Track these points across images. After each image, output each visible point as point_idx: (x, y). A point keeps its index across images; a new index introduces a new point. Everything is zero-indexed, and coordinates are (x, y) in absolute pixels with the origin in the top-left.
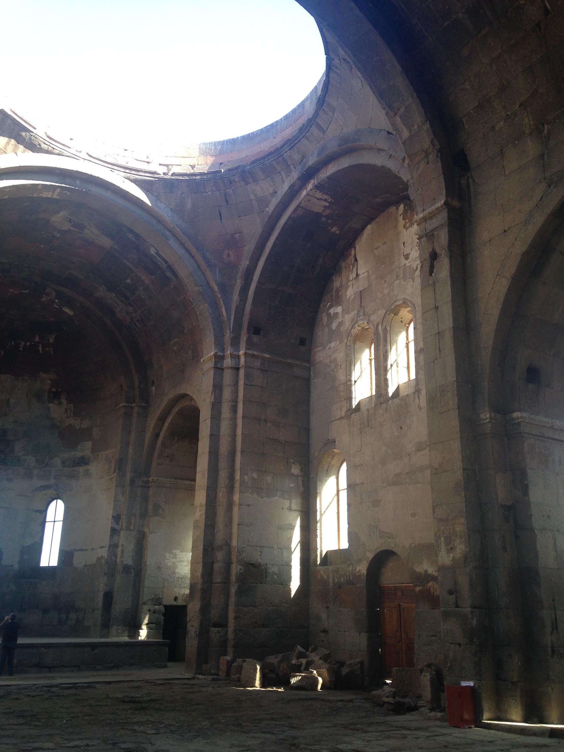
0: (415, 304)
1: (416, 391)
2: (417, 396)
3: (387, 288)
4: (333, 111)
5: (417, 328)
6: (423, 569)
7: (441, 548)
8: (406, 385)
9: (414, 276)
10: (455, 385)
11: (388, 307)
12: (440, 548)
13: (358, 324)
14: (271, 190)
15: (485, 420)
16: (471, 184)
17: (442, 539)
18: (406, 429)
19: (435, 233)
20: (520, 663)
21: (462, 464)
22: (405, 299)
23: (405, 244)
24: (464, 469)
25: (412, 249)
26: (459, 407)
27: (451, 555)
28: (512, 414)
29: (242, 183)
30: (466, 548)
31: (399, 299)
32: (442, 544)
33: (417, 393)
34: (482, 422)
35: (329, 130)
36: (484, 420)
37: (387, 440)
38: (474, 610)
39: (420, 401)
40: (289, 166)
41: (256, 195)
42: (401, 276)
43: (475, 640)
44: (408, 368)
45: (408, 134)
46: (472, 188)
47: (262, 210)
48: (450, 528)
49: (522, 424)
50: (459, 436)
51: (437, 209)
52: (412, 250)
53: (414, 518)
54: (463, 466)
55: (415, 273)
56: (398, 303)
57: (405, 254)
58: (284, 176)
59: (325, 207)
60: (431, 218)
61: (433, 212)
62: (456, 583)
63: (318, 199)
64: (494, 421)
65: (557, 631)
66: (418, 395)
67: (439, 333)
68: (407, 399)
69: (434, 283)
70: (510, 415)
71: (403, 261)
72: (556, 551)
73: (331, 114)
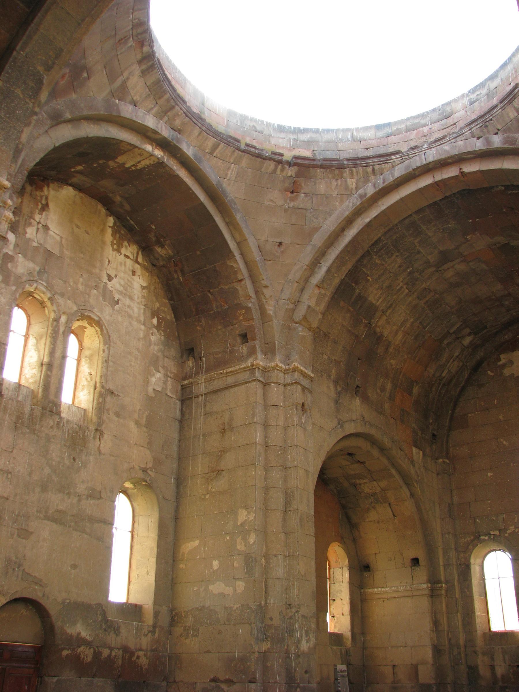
4: (235, 163)
13: (37, 286)
14: (137, 98)
17: (304, 631)
18: (80, 465)
27: (308, 644)
29: (139, 56)
31: (94, 313)
35: (215, 159)
37: (54, 463)
39: (100, 444)
40: (166, 113)
41: (128, 79)
45: (314, 305)
47: (114, 95)
53: (74, 569)
56: (93, 316)
58: (155, 110)
59: (124, 164)
63: (139, 162)
71: (105, 280)
73: (232, 161)
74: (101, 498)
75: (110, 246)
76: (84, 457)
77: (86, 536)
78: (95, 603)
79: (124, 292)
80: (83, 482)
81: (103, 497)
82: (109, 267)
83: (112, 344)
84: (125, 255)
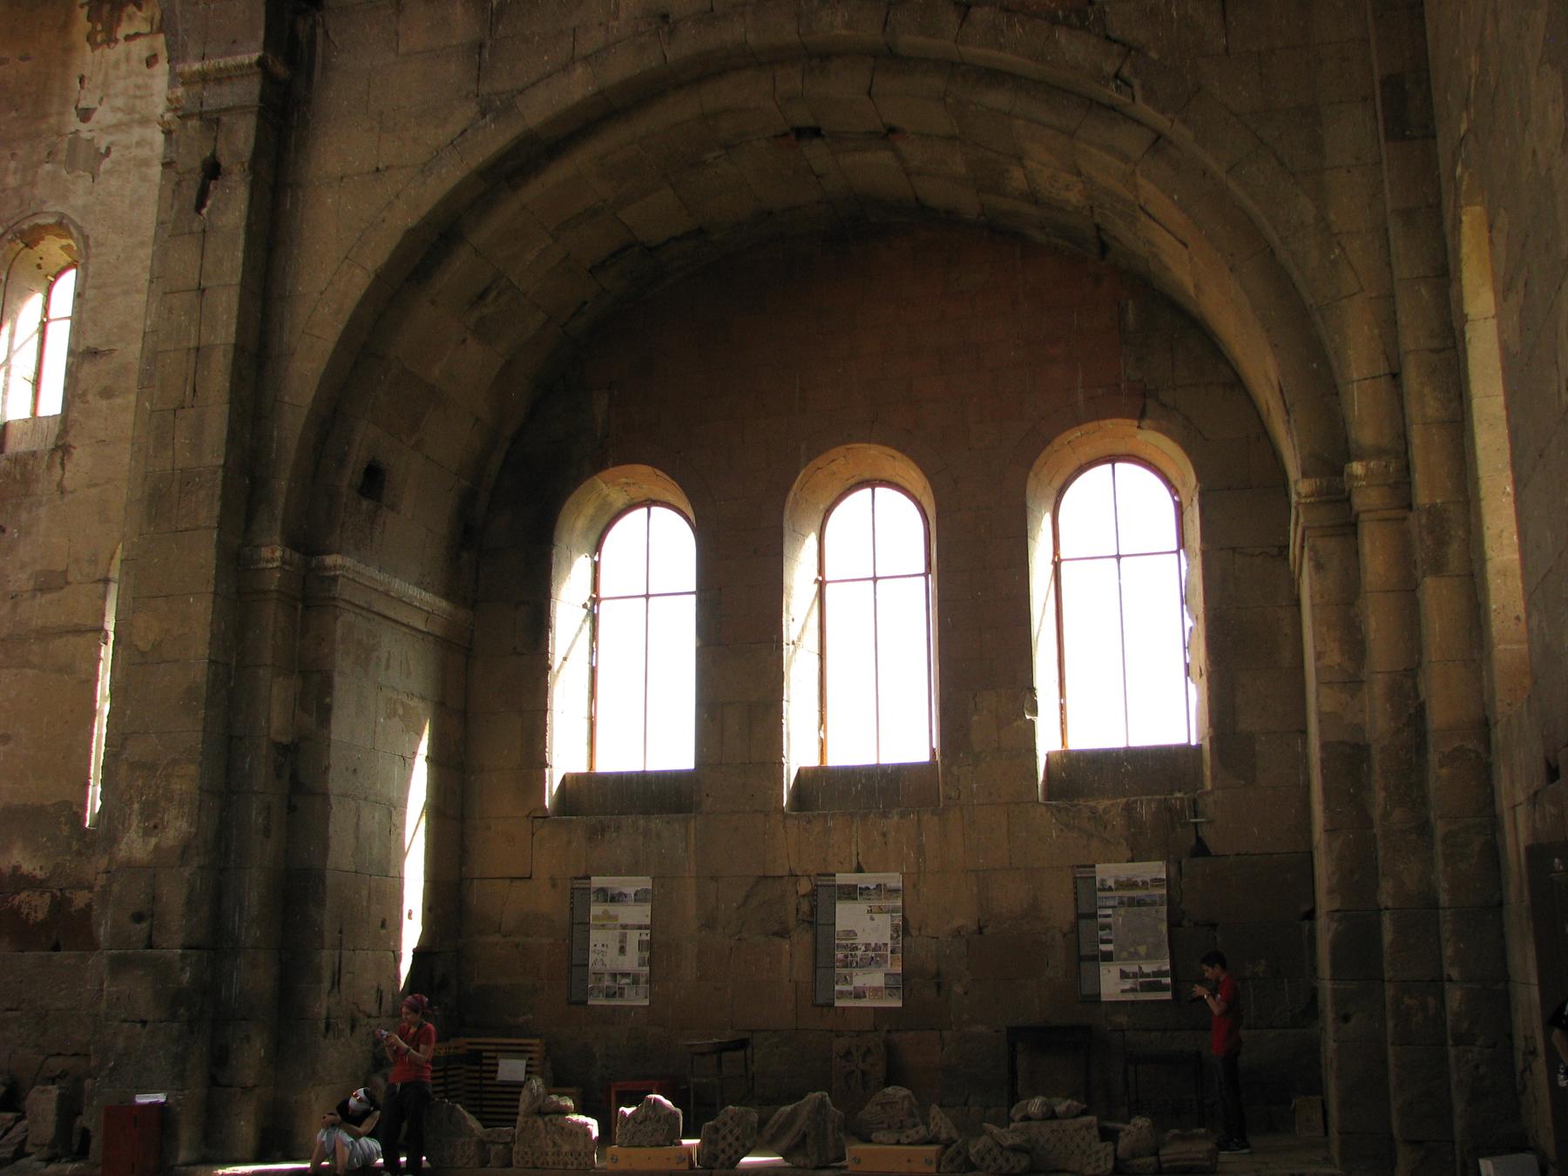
0: (88, 236)
1: (56, 448)
2: (58, 460)
3: (15, 172)
5: (87, 296)
6: (9, 862)
7: (130, 826)
8: (26, 425)
9: (98, 170)
10: (220, 473)
11: (11, 224)
12: (126, 825)
15: (271, 562)
16: (320, 39)
17: (136, 806)
18: (16, 535)
19: (225, 119)
20: (262, 1051)
21: (208, 651)
22: (63, 216)
23: (86, 81)
24: (211, 662)
25: (102, 99)
26: (220, 527)
27: (153, 841)
28: (324, 557)
30: (191, 825)
31: (46, 212)
32: (133, 817)
33: (60, 454)
34: (263, 565)
36: (267, 561)
38: (189, 952)
39: (64, 474)
42: (62, 156)
43: (182, 1011)
44: (37, 383)
46: (319, 50)
48: (158, 782)
49: (340, 580)
50: (211, 589)
51: (240, 67)
52: (103, 103)
54: (210, 655)
55: (100, 163)
56: (41, 221)
57: (80, 106)
60: (219, 81)
61: (226, 69)
62: (154, 899)
64: (287, 568)
65: (339, 989)
66: (62, 459)
67: (198, 349)
68: (31, 462)
69: (204, 231)
70: (320, 558)
71: (73, 122)
72: (357, 838)
74: (67, 583)
75: (88, 45)
76: (24, 516)
77: (30, 672)
78: (54, 801)
79: (125, 118)
80: (23, 567)
81: (71, 580)
82: (83, 92)
83: (94, 251)
84: (128, 38)
